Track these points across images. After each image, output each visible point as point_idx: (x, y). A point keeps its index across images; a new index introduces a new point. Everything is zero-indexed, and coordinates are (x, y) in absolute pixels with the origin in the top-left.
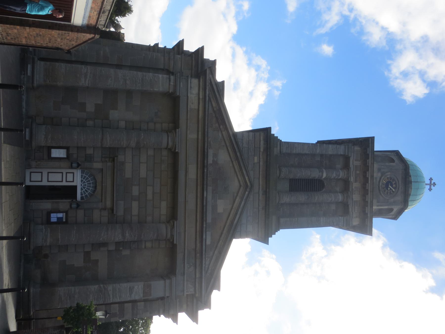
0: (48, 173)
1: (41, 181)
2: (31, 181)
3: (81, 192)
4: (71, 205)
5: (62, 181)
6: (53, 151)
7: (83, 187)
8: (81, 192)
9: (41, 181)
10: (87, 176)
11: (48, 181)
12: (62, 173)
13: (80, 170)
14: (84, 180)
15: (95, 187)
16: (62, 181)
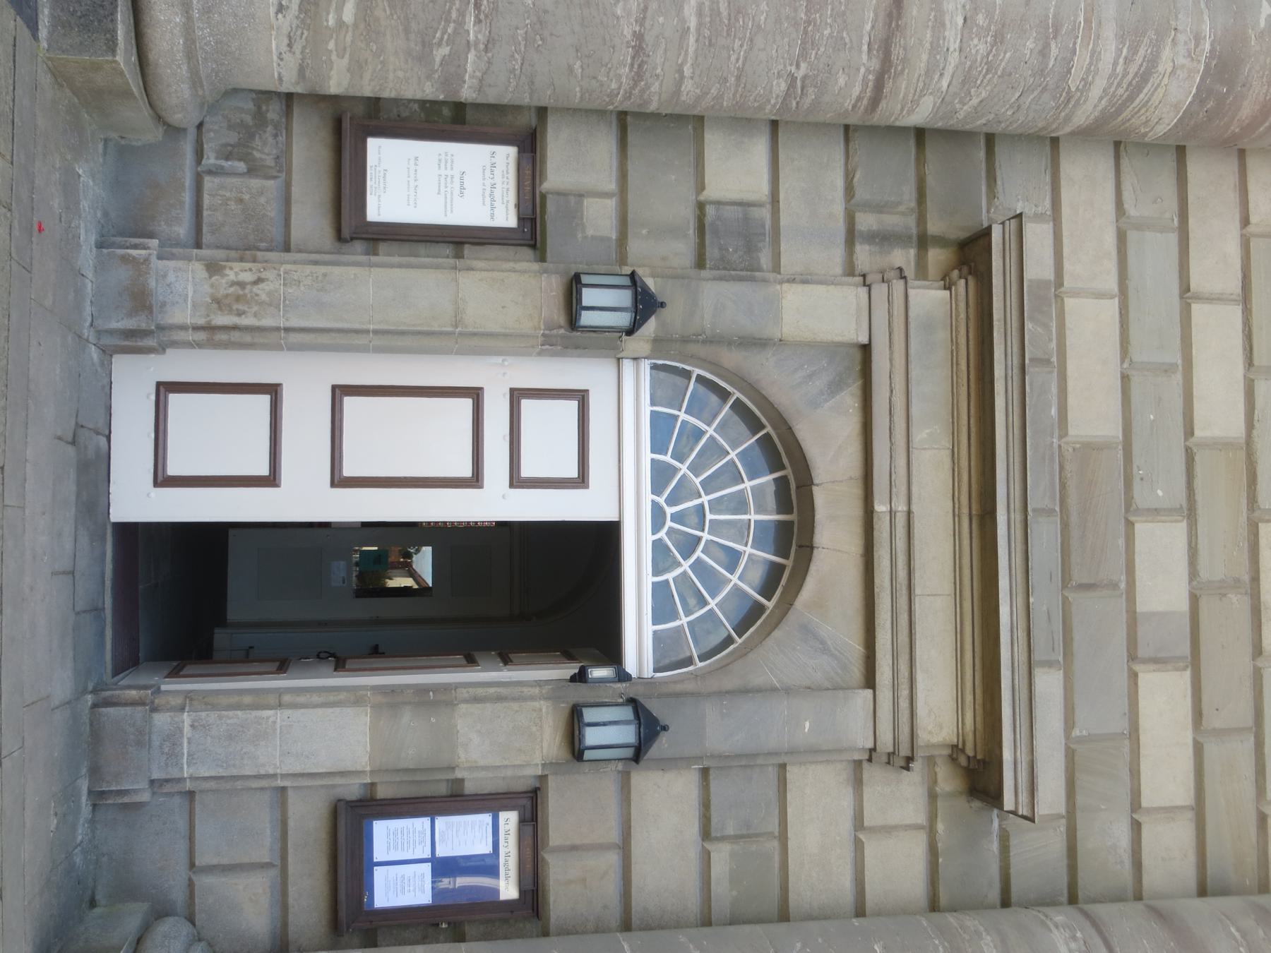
0: (340, 392)
1: (271, 480)
4: (574, 722)
5: (475, 480)
7: (671, 532)
8: (660, 591)
9: (271, 480)
10: (711, 431)
11: (339, 481)
12: (475, 394)
16: (475, 480)
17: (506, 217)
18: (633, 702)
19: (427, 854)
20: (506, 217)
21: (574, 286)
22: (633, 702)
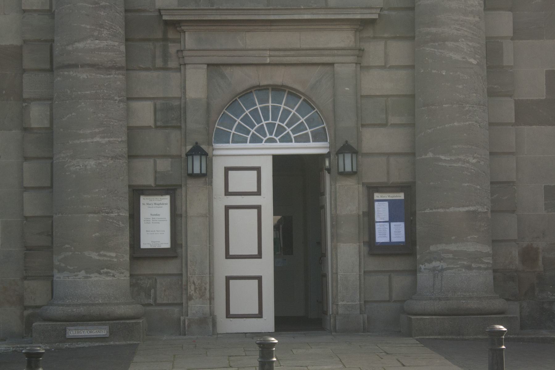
0: (228, 256)
1: (259, 279)
2: (260, 315)
3: (296, 142)
4: (344, 174)
5: (259, 208)
6: (146, 242)
8: (298, 140)
9: (259, 279)
11: (259, 256)
12: (227, 208)
13: (216, 146)
14: (253, 131)
15: (278, 89)
16: (259, 208)
17: (166, 199)
18: (338, 153)
19: (387, 224)
20: (166, 199)
21: (193, 176)
22: (338, 153)
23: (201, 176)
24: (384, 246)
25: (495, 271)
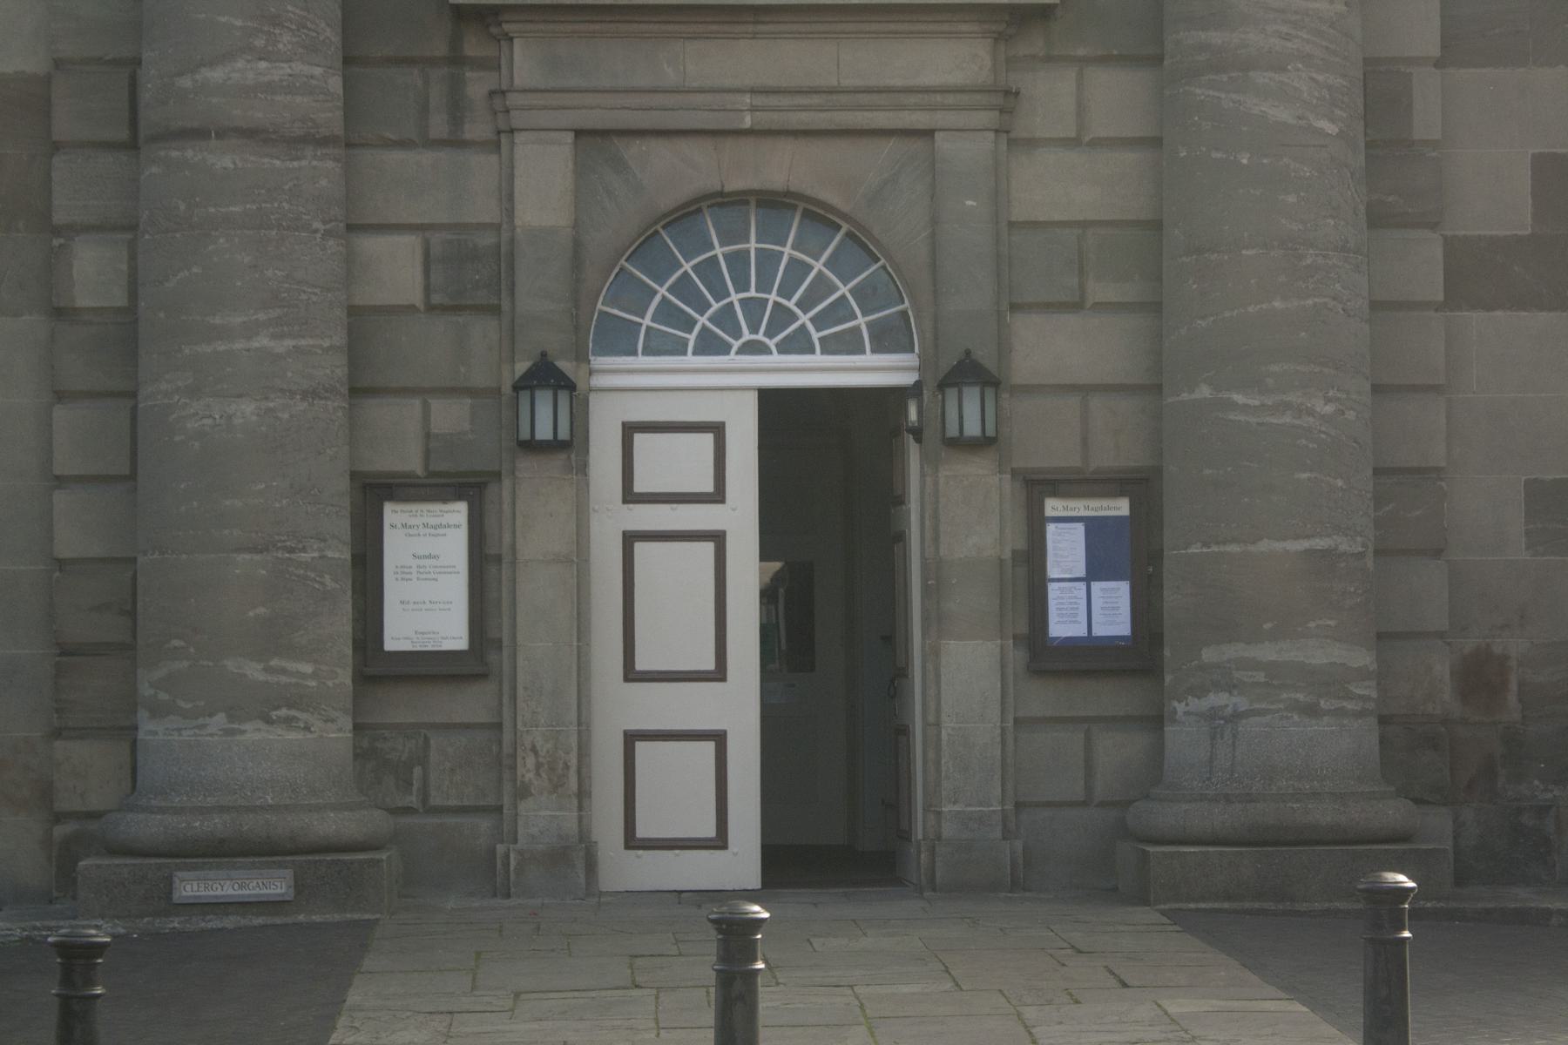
0: (631, 674)
1: (719, 739)
2: (720, 842)
9: (719, 739)
11: (719, 673)
12: (630, 539)
13: (599, 362)
14: (703, 320)
15: (775, 203)
17: (457, 513)
19: (1082, 586)
20: (457, 513)
21: (532, 446)
22: (942, 386)
23: (556, 446)
24: (1070, 646)
25: (1383, 720)
